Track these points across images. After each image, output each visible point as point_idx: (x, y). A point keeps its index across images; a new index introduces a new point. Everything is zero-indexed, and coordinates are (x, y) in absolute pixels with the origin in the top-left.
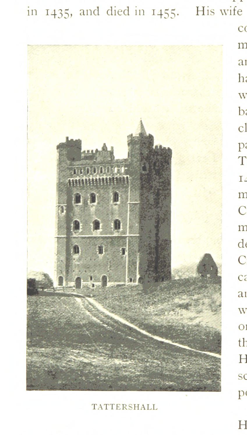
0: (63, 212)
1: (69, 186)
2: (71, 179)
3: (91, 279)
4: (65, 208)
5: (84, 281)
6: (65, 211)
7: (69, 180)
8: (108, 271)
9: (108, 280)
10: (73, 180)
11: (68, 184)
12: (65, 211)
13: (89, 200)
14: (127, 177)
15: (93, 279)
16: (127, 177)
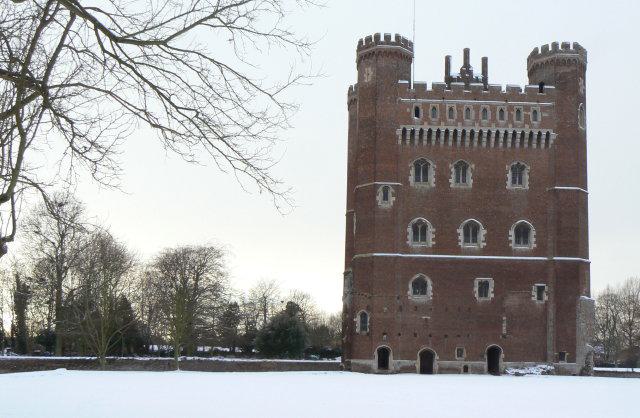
0: (386, 198)
1: (400, 142)
2: (409, 129)
3: (460, 355)
4: (391, 190)
5: (441, 359)
6: (392, 199)
7: (404, 131)
8: (504, 336)
9: (502, 356)
10: (413, 132)
11: (400, 137)
12: (392, 199)
13: (453, 176)
14: (548, 134)
15: (465, 355)
16: (548, 134)
